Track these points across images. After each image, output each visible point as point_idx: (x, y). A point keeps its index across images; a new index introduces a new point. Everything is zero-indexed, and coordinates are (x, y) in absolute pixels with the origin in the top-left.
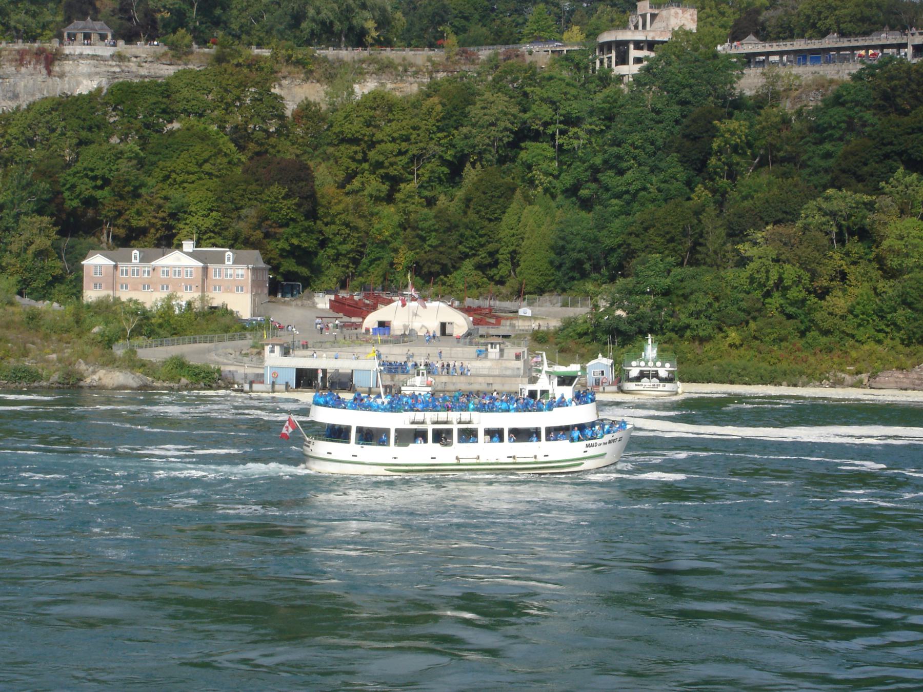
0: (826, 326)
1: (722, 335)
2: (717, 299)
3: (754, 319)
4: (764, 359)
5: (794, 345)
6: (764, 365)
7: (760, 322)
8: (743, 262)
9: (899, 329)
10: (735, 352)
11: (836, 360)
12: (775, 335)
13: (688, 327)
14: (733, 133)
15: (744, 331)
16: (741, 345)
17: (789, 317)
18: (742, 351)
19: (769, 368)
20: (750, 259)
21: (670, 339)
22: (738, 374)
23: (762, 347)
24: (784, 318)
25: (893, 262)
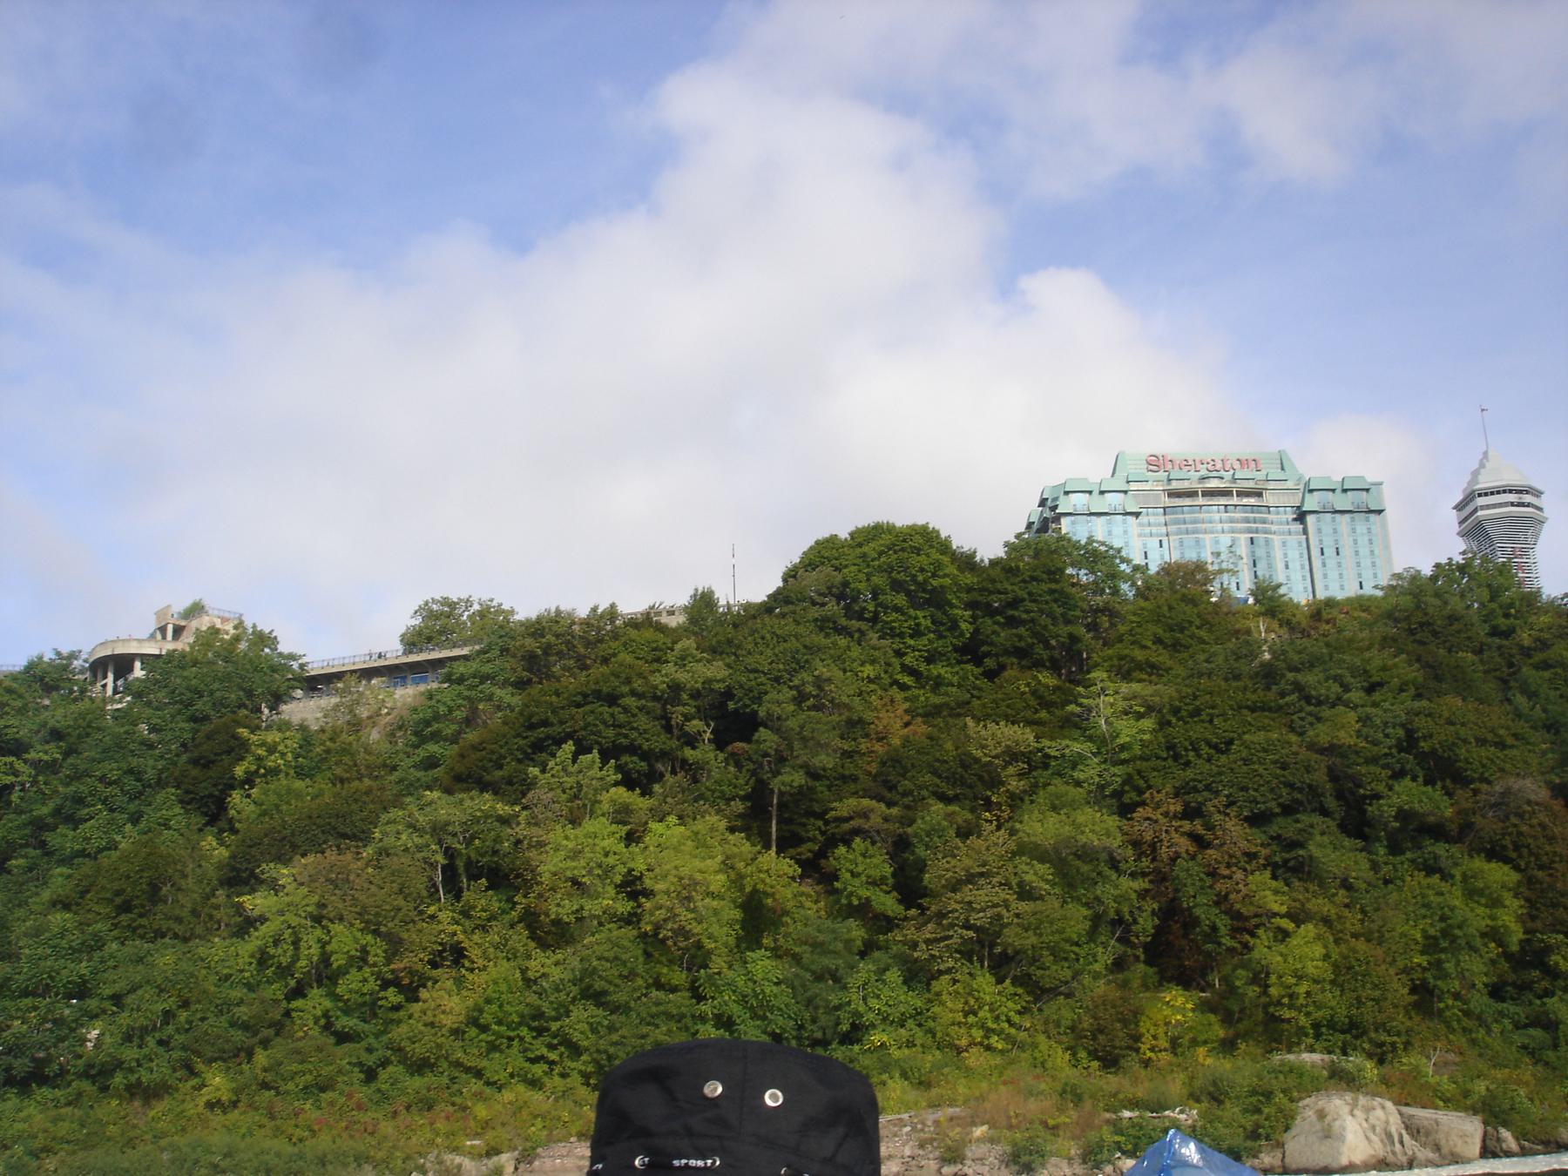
0: (419, 1050)
1: (195, 1082)
2: (185, 1004)
3: (265, 1043)
4: (279, 1130)
5: (350, 1096)
6: (280, 1144)
7: (279, 1048)
8: (247, 925)
9: (575, 1050)
10: (217, 1119)
11: (441, 1125)
12: (309, 1077)
13: (118, 1065)
14: (272, 749)
15: (241, 1073)
16: (235, 1104)
17: (343, 1038)
18: (234, 1115)
19: (290, 1149)
20: (262, 919)
21: (80, 1095)
22: (216, 1166)
23: (279, 1105)
24: (332, 1040)
25: (562, 907)
